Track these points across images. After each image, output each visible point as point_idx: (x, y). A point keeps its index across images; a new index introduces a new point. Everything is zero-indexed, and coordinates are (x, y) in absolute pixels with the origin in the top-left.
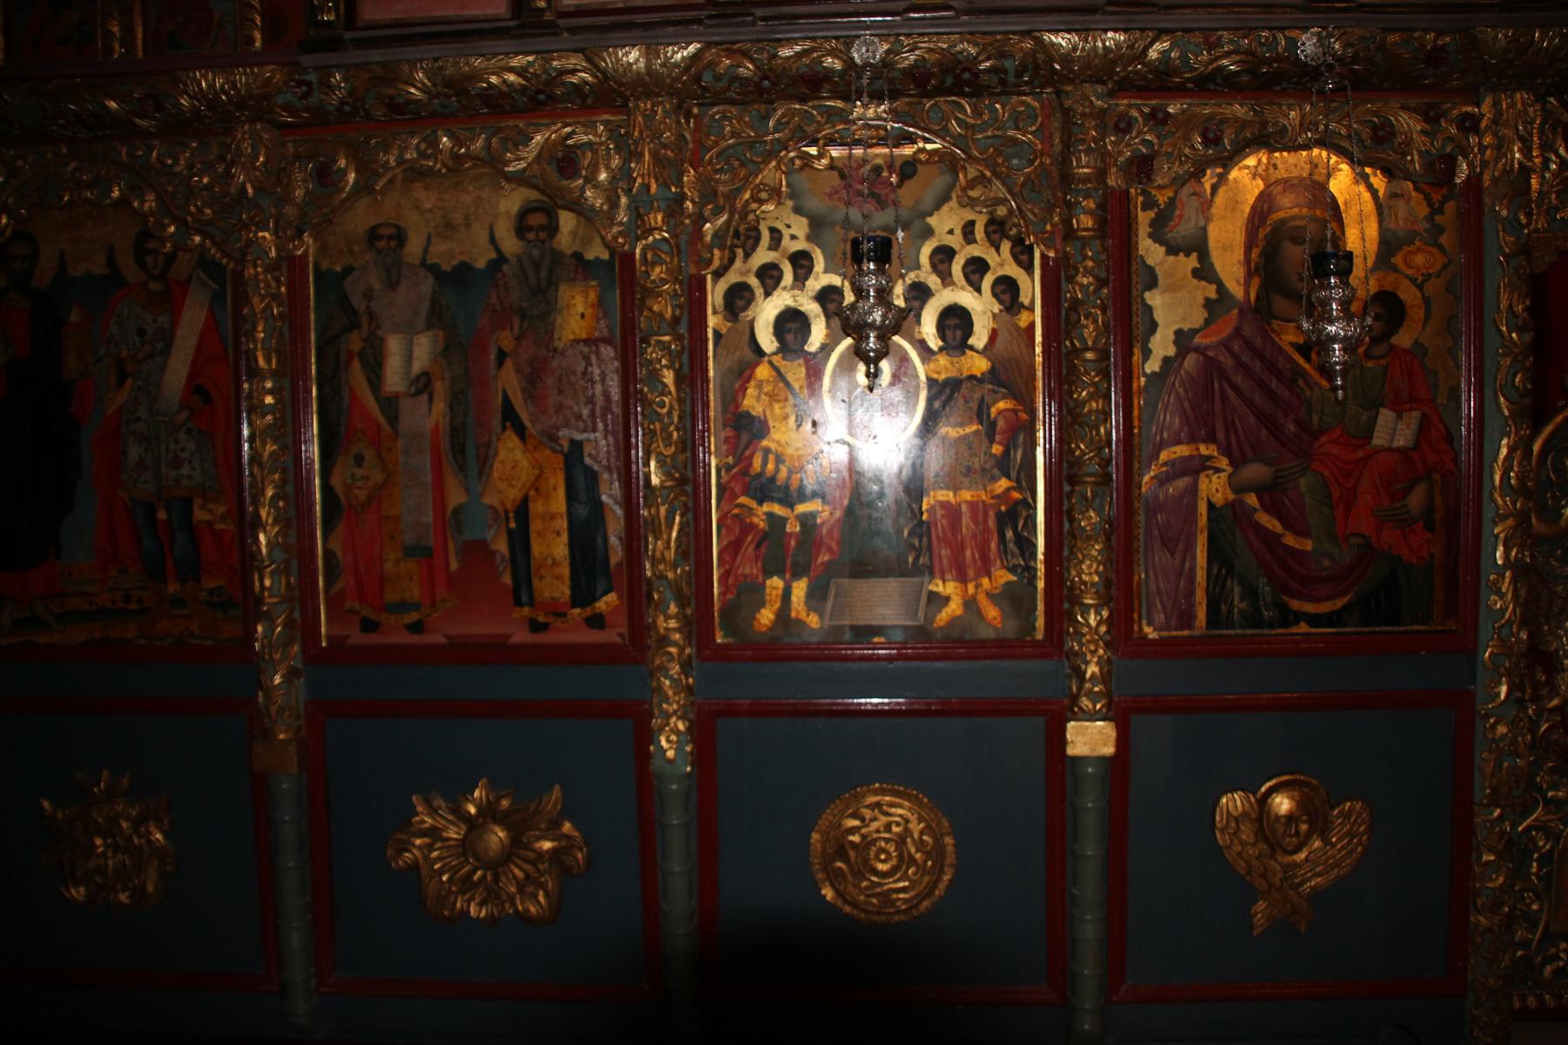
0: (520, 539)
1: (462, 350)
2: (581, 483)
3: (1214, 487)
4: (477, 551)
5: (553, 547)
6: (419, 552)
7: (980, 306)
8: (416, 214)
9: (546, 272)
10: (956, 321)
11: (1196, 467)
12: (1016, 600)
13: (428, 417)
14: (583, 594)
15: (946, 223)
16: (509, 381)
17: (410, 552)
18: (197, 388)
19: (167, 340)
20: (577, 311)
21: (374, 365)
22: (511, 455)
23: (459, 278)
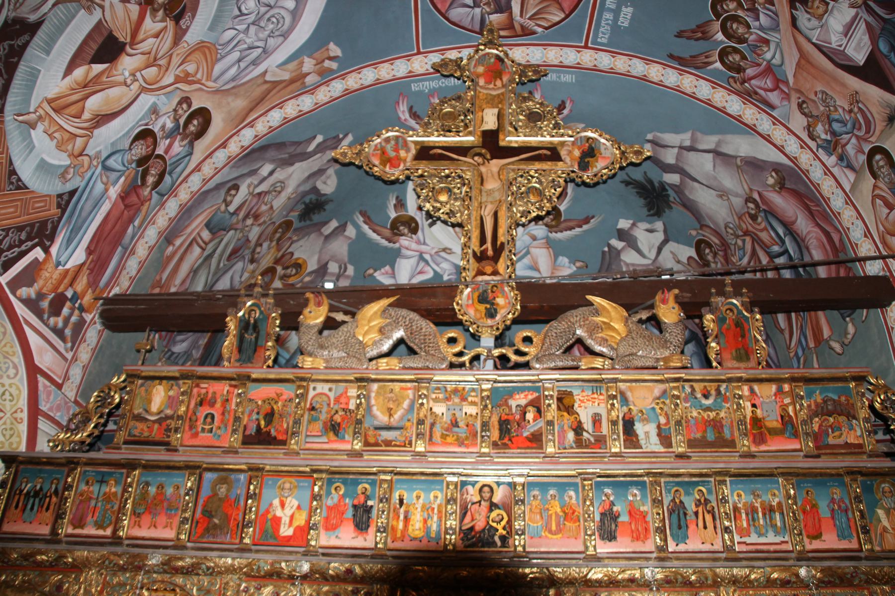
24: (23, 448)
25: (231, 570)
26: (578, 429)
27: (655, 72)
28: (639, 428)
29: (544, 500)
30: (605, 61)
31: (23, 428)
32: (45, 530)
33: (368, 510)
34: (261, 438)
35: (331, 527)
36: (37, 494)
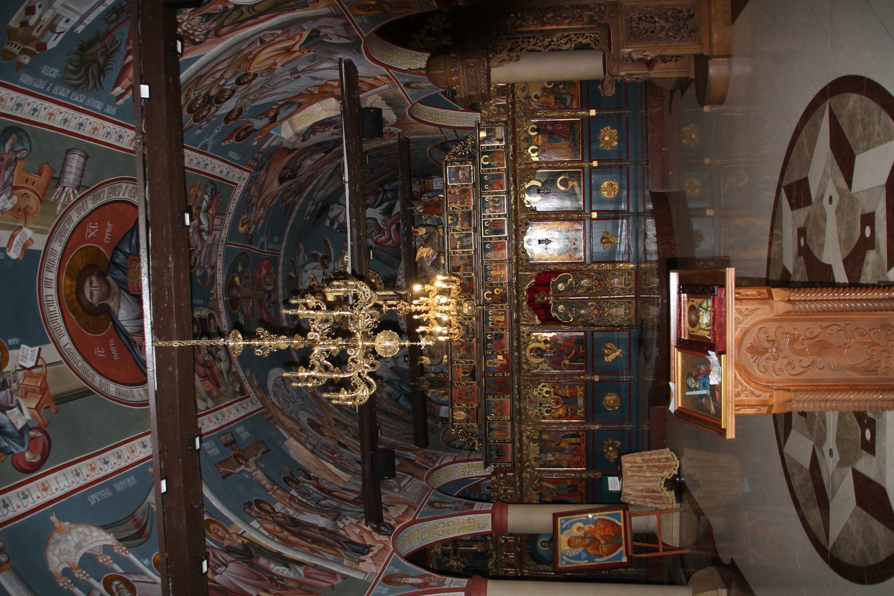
0: (573, 444)
1: (550, 450)
2: (566, 437)
3: (567, 362)
4: (574, 449)
5: (574, 440)
6: (574, 456)
7: (545, 389)
8: (533, 456)
9: (540, 440)
10: (547, 392)
11: (564, 364)
12: (580, 386)
13: (558, 455)
14: (579, 437)
15: (535, 393)
16: (553, 445)
17: (574, 456)
18: (553, 484)
19: (548, 487)
20: (545, 437)
21: (551, 461)
22: (562, 445)
23: (541, 451)
24: (482, 462)
25: (519, 378)
26: (466, 265)
27: (291, 222)
28: (465, 244)
29: (491, 276)
30: (284, 244)
31: (474, 463)
32: (510, 445)
33: (496, 335)
34: (473, 376)
35: (503, 347)
36: (498, 452)
